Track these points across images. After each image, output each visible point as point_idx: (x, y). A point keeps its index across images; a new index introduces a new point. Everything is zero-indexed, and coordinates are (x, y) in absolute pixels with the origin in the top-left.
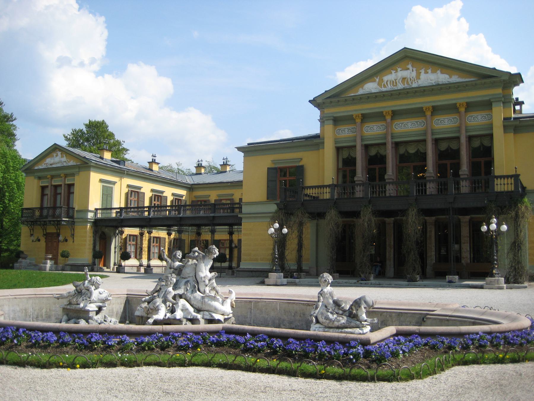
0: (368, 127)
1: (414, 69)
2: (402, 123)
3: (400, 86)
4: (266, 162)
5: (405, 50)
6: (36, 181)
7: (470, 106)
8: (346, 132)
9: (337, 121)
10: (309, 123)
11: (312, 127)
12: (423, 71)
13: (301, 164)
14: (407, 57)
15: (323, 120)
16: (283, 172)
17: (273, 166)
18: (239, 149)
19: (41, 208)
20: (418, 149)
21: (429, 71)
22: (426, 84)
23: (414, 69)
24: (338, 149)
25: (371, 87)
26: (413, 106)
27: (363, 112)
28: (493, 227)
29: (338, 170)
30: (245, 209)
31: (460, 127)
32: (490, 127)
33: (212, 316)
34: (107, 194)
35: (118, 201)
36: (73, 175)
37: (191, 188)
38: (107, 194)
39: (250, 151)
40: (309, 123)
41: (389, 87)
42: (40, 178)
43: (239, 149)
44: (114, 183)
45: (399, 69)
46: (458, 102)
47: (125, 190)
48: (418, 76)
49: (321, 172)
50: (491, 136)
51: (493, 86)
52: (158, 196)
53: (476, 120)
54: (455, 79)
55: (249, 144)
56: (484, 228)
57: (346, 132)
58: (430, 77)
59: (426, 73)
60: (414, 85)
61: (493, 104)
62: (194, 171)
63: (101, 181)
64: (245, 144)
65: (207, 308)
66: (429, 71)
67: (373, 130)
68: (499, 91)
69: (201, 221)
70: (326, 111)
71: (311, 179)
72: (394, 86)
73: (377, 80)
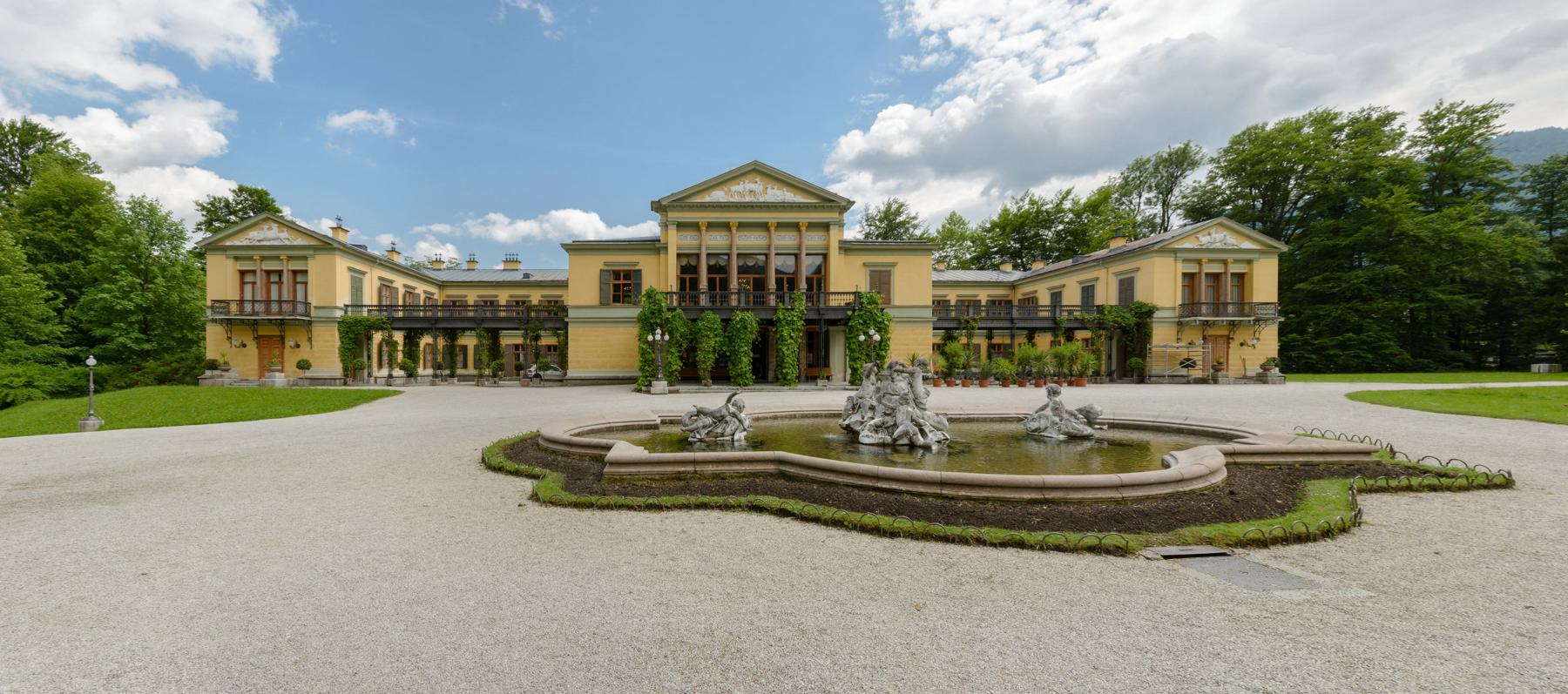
5: (756, 163)
6: (231, 262)
8: (688, 240)
11: (649, 228)
19: (242, 302)
24: (679, 256)
25: (718, 196)
28: (658, 337)
30: (571, 313)
32: (827, 248)
34: (357, 288)
35: (370, 297)
36: (305, 258)
37: (442, 285)
38: (357, 288)
41: (737, 199)
42: (236, 258)
44: (364, 273)
47: (377, 284)
49: (660, 276)
50: (825, 256)
51: (831, 209)
52: (410, 292)
56: (862, 338)
57: (688, 240)
62: (465, 266)
63: (350, 269)
67: (716, 241)
68: (836, 215)
69: (464, 330)
70: (671, 215)
71: (648, 282)
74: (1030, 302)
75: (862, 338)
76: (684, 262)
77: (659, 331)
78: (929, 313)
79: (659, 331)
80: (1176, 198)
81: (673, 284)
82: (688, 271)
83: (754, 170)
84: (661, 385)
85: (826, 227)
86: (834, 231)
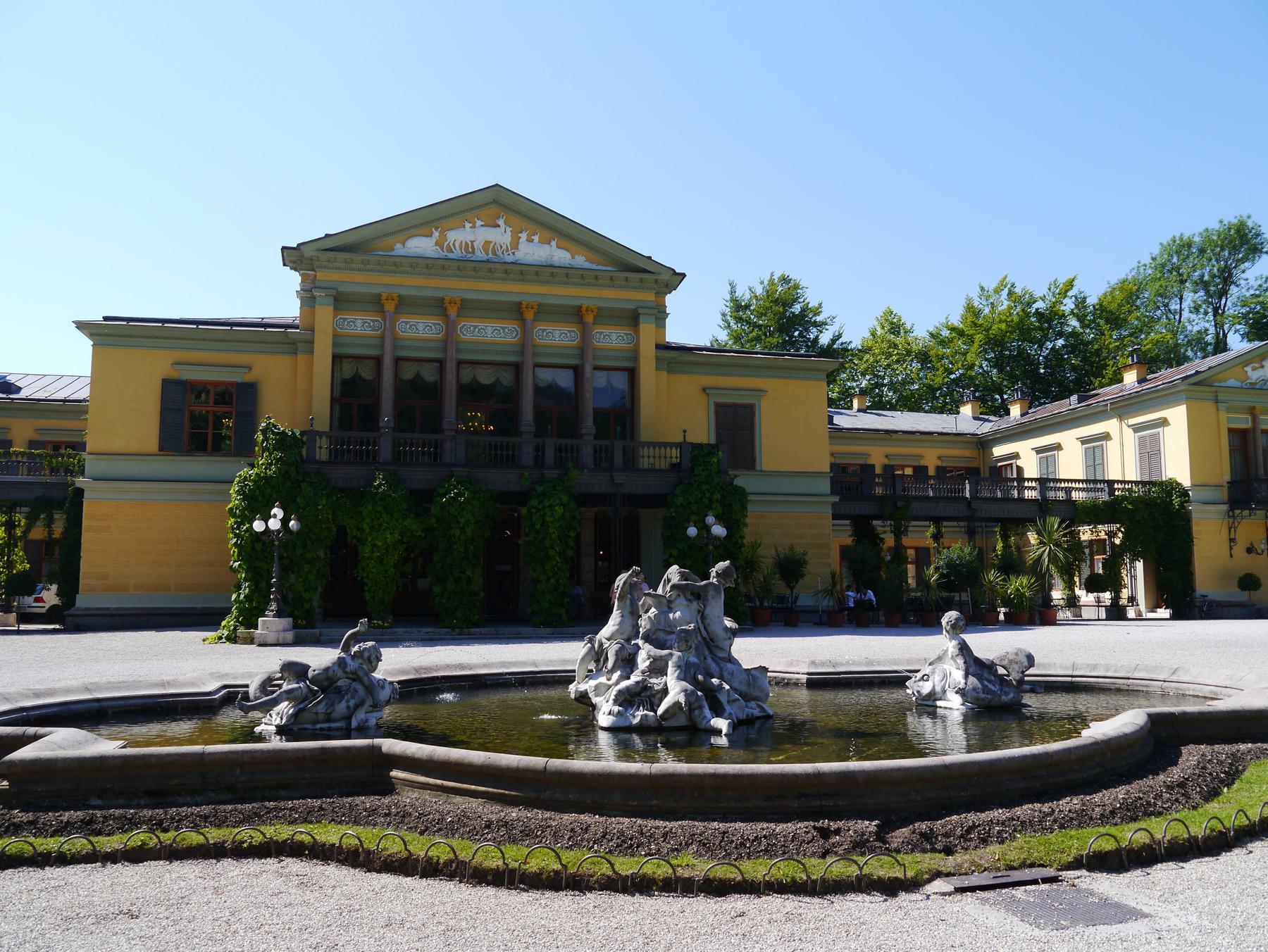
0: (407, 323)
1: (509, 230)
2: (475, 327)
3: (480, 255)
4: (154, 368)
7: (606, 315)
8: (360, 325)
9: (341, 301)
10: (277, 297)
12: (524, 236)
13: (248, 378)
14: (497, 203)
15: (308, 297)
16: (198, 392)
17: (174, 375)
18: (81, 325)
20: (498, 379)
21: (536, 238)
22: (530, 259)
23: (509, 230)
24: (336, 358)
25: (421, 245)
26: (503, 298)
27: (404, 292)
29: (333, 400)
31: (382, 337)
32: (635, 355)
33: (763, 709)
39: (109, 335)
40: (277, 297)
43: (81, 325)
45: (479, 223)
46: (586, 304)
48: (515, 244)
49: (295, 401)
50: (632, 373)
51: (641, 285)
53: (610, 338)
54: (580, 261)
55: (106, 319)
56: (692, 531)
58: (534, 251)
59: (530, 240)
60: (510, 259)
61: (642, 318)
64: (96, 316)
65: (756, 693)
66: (536, 238)
68: (650, 297)
70: (320, 275)
72: (468, 252)
73: (436, 234)
74: (1001, 474)
75: (692, 531)
76: (348, 370)
77: (277, 512)
78: (825, 486)
79: (277, 512)
80: (1231, 304)
81: (321, 412)
82: (354, 394)
83: (495, 202)
84: (269, 624)
85: (632, 318)
86: (646, 329)
